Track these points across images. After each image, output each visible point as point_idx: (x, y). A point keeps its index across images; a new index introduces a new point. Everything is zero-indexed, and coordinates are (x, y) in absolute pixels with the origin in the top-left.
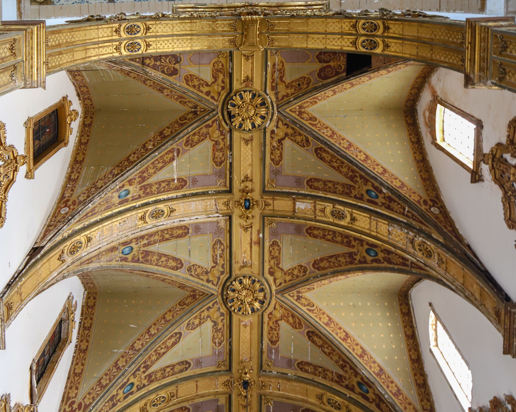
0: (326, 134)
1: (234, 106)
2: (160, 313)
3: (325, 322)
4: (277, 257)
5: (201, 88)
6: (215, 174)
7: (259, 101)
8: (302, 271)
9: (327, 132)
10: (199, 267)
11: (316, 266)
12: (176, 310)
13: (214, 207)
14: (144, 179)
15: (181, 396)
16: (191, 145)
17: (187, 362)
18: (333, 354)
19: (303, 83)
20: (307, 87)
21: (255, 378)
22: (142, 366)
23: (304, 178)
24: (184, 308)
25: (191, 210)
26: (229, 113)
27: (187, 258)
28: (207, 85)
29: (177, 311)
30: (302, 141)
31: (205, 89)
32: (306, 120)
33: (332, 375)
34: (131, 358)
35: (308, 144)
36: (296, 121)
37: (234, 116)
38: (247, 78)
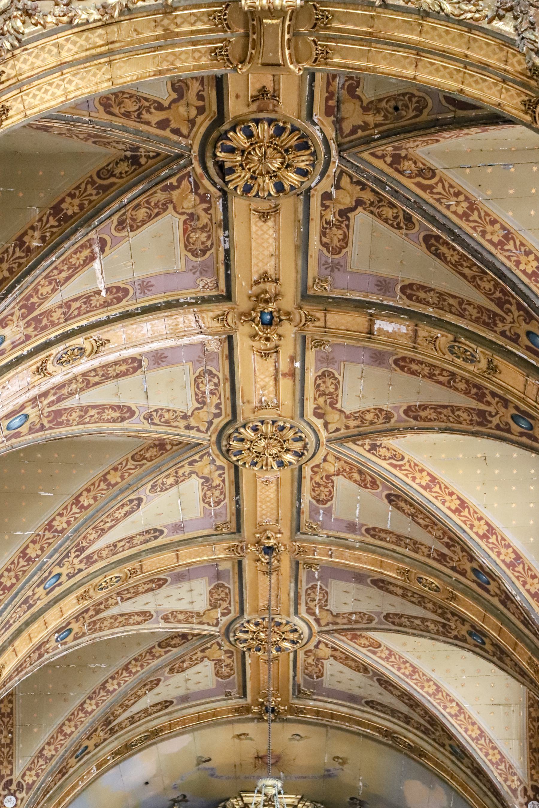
0: (453, 208)
1: (232, 150)
2: (96, 473)
3: (424, 483)
4: (331, 394)
5: (146, 116)
6: (193, 270)
7: (294, 141)
8: (381, 418)
9: (458, 203)
10: (168, 411)
11: (411, 413)
12: (128, 467)
13: (194, 324)
14: (31, 308)
15: (149, 569)
16: (131, 226)
17: (155, 530)
18: (432, 528)
19: (407, 107)
20: (416, 116)
21: (286, 541)
22: (73, 551)
23: (397, 282)
24: (143, 465)
25: (144, 335)
26: (220, 166)
27: (144, 402)
28: (160, 107)
29: (130, 469)
30: (396, 218)
31: (157, 116)
32: (410, 177)
33: (429, 551)
34: (50, 544)
35: (410, 225)
36: (384, 179)
37: (232, 171)
38: (263, 91)
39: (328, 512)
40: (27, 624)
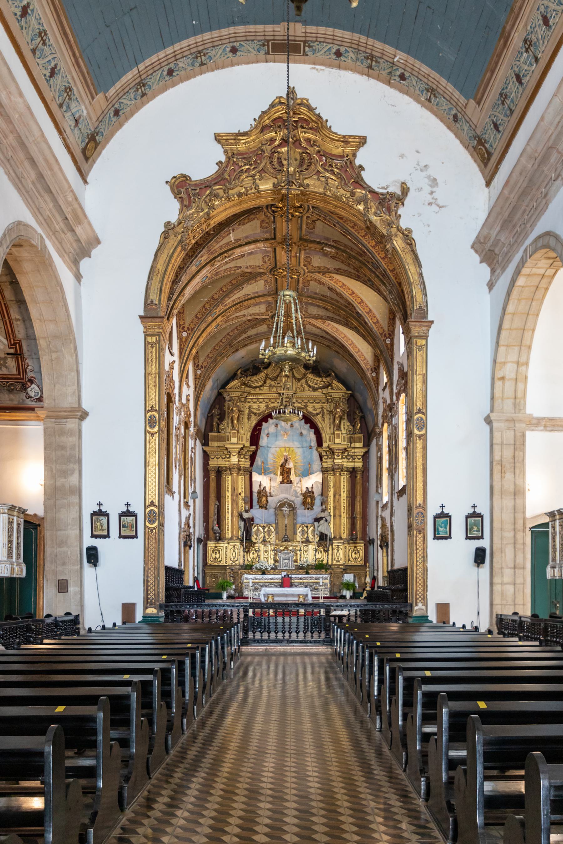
39: (308, 289)
40: (206, 328)
